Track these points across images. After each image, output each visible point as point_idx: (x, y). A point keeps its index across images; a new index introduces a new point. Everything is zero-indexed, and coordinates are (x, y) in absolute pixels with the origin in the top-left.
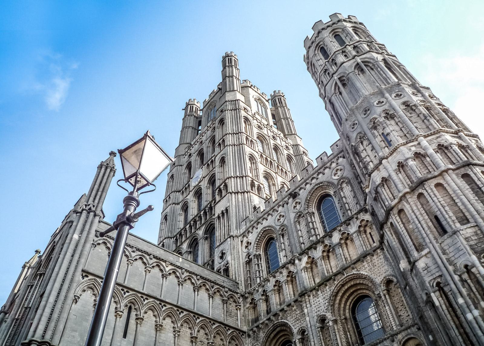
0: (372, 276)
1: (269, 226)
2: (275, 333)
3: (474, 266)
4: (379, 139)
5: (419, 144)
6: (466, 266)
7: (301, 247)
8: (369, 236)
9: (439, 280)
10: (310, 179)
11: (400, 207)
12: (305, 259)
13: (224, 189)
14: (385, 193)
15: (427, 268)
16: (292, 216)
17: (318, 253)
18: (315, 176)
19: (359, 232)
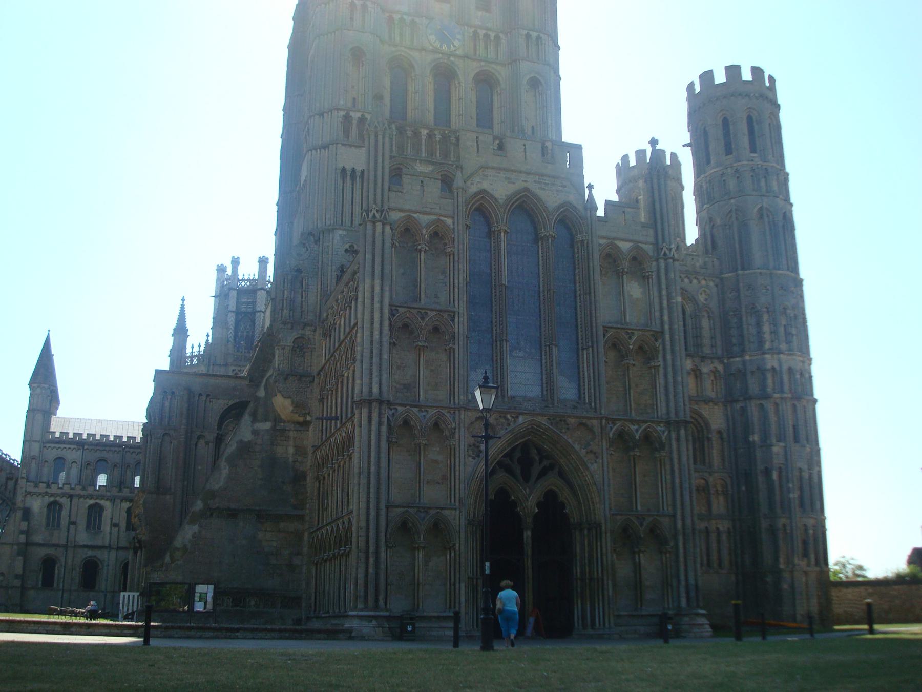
4: (782, 329)
9: (782, 466)
11: (778, 401)
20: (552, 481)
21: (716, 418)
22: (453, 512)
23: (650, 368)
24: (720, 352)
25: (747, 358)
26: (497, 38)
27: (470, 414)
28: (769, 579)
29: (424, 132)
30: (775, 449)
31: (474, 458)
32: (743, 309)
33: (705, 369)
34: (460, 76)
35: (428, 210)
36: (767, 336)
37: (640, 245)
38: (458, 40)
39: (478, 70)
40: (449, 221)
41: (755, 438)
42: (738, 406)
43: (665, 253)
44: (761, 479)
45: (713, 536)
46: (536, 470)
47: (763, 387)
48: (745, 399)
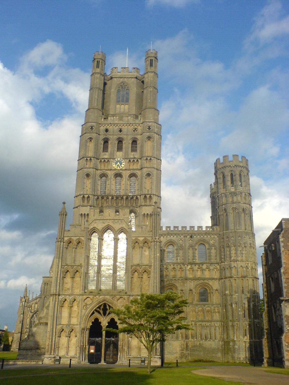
0: (213, 286)
1: (174, 241)
2: (168, 285)
3: (246, 304)
5: (248, 263)
6: (244, 303)
7: (188, 261)
8: (215, 272)
10: (201, 235)
11: (236, 278)
12: (189, 267)
13: (148, 199)
14: (234, 271)
15: (235, 298)
16: (187, 245)
17: (196, 268)
18: (203, 235)
19: (213, 270)
20: (113, 316)
21: (215, 285)
22: (77, 326)
23: (149, 277)
24: (218, 261)
25: (226, 263)
26: (137, 161)
27: (84, 296)
28: (231, 344)
29: (110, 197)
30: (234, 296)
31: (85, 310)
32: (225, 245)
33: (211, 268)
34: (124, 176)
35: (77, 235)
36: (233, 255)
37: (147, 238)
38: (123, 164)
39: (130, 173)
40: (83, 238)
41: (227, 292)
42: (223, 280)
43: (154, 240)
44: (229, 307)
45: (213, 329)
46: (108, 312)
47: (231, 273)
48: (225, 278)
